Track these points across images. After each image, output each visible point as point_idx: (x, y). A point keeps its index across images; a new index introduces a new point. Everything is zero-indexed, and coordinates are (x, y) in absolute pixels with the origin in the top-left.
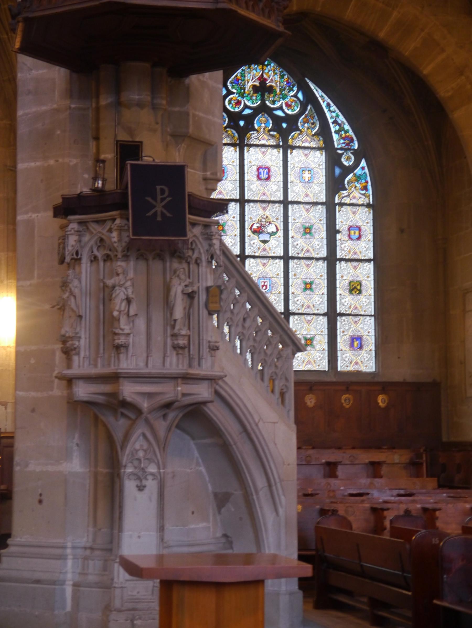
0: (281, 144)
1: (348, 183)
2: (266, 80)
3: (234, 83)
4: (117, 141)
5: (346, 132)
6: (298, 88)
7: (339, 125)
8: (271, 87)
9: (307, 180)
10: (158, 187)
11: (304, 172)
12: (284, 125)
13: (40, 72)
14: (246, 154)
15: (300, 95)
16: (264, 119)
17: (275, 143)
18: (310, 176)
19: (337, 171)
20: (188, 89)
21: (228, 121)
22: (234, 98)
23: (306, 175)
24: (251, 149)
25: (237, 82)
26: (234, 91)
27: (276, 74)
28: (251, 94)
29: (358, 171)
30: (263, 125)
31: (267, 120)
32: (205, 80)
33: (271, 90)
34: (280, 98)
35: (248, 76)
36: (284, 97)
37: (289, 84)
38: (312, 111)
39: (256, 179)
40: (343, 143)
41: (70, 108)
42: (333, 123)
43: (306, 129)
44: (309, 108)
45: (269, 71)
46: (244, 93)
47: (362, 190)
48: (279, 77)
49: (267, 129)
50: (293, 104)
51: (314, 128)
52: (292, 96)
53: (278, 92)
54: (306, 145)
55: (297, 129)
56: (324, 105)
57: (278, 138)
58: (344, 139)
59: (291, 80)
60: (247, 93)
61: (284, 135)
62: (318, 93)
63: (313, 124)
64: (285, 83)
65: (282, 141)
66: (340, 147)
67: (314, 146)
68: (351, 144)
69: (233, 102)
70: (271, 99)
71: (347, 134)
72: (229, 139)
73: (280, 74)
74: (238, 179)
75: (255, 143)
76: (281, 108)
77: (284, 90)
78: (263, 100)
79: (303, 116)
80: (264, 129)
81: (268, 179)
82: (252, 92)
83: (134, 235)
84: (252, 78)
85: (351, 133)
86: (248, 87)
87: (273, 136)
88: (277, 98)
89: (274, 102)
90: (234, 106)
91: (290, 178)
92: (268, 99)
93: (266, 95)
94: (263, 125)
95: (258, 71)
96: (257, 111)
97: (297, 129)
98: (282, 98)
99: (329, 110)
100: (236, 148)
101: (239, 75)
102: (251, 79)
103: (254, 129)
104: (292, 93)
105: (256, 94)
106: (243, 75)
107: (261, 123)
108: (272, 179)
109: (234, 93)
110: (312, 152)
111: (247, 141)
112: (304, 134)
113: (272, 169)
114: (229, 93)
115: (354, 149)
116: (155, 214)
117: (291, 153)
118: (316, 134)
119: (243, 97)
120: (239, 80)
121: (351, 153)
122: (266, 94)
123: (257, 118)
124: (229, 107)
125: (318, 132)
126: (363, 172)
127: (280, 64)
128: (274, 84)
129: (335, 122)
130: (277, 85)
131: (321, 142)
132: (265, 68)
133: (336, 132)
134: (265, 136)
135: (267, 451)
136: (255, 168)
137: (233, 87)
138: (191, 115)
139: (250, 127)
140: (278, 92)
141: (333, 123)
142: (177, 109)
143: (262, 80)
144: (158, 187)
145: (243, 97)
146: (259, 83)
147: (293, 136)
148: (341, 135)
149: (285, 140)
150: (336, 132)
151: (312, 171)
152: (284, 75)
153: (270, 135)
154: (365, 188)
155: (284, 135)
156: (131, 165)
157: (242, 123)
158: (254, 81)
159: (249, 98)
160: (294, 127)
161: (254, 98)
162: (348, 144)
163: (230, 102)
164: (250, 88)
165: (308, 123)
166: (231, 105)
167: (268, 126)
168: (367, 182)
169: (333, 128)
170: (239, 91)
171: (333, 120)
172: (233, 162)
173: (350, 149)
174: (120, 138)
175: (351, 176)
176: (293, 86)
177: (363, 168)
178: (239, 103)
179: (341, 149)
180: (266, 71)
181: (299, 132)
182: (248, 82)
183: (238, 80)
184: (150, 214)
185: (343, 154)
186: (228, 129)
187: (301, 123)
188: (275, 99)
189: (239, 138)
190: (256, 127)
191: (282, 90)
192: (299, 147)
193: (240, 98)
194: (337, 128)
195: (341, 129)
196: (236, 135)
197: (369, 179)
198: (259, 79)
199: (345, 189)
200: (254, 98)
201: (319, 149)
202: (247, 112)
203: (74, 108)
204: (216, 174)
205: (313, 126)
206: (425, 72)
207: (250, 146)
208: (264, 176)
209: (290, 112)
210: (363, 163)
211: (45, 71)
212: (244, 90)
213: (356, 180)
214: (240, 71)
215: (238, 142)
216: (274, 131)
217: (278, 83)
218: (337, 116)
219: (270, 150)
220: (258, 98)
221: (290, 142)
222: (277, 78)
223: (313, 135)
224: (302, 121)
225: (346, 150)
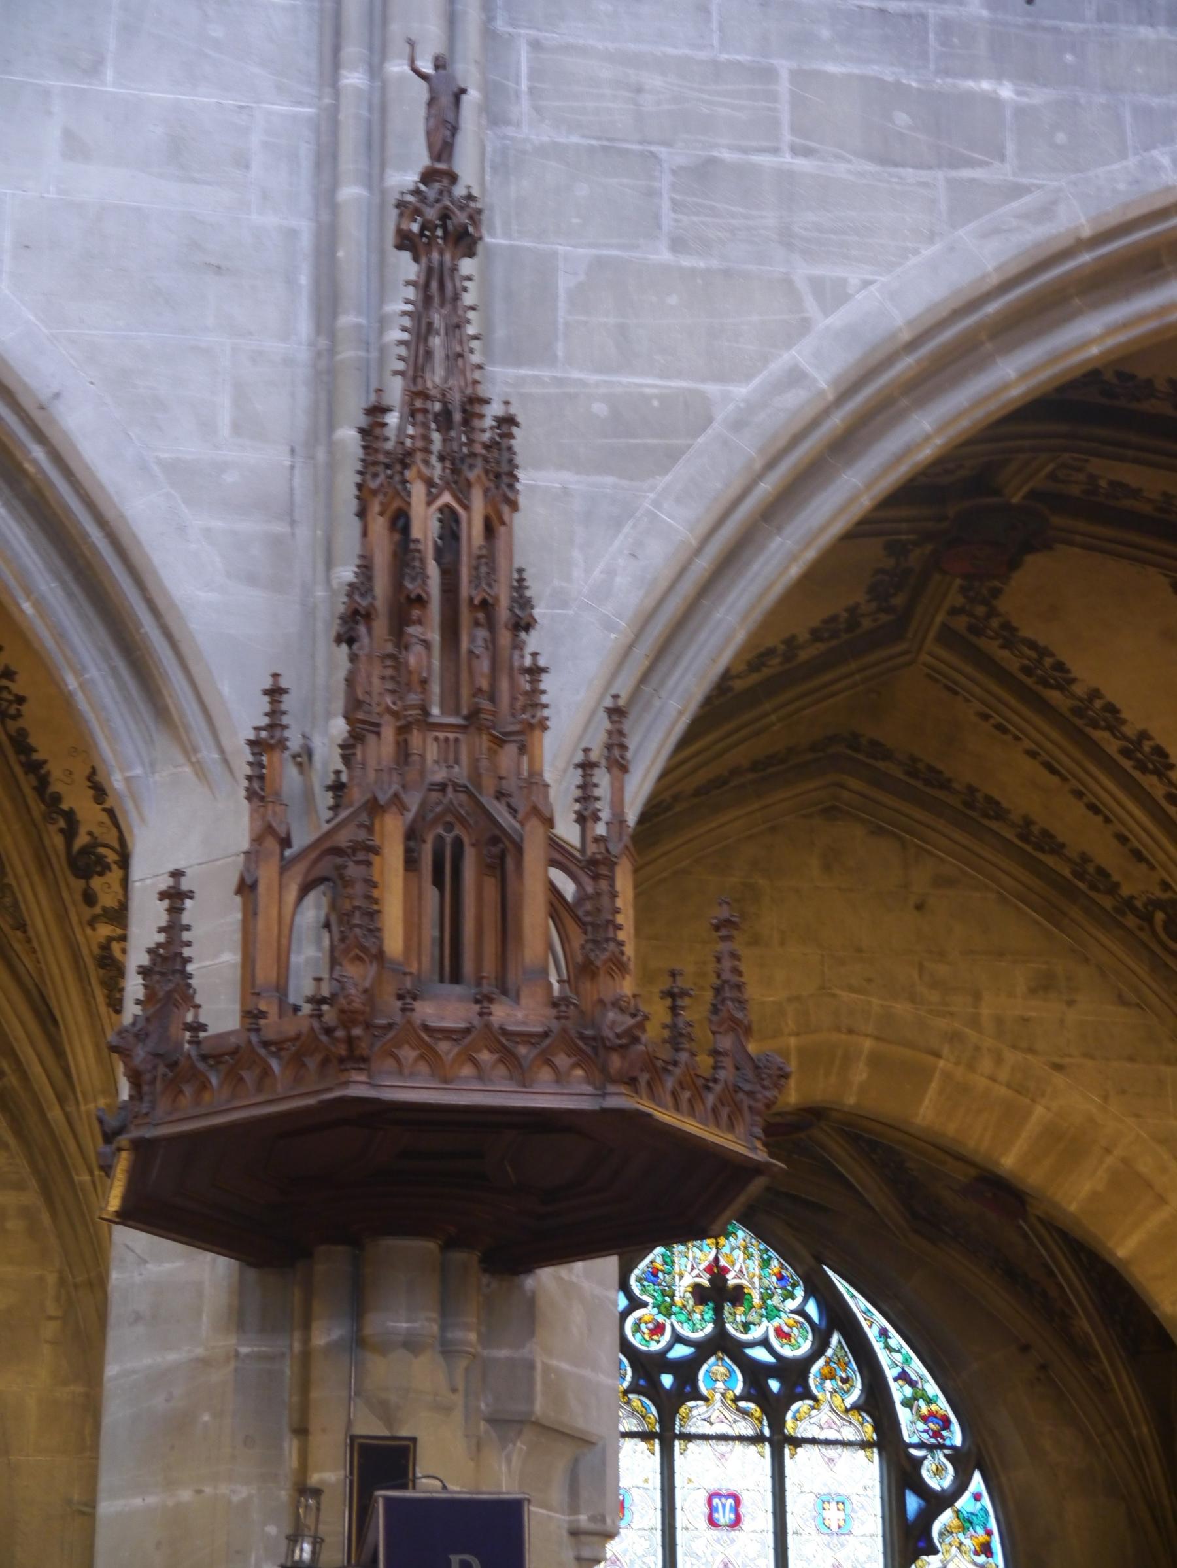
0: (767, 1432)
1: (941, 1534)
2: (725, 1270)
3: (646, 1280)
4: (353, 1438)
5: (929, 1401)
6: (805, 1291)
7: (912, 1384)
8: (739, 1288)
9: (835, 1528)
11: (826, 1506)
12: (774, 1385)
13: (167, 1266)
14: (679, 1460)
15: (812, 1309)
16: (722, 1370)
17: (750, 1432)
18: (841, 1515)
19: (913, 1503)
20: (531, 1303)
21: (633, 1378)
22: (647, 1318)
23: (833, 1515)
24: (691, 1445)
25: (652, 1278)
26: (645, 1298)
27: (750, 1256)
28: (689, 1308)
29: (965, 1503)
30: (720, 1385)
31: (731, 1372)
32: (574, 1279)
33: (738, 1296)
34: (762, 1316)
36: (771, 1313)
37: (783, 1282)
38: (842, 1347)
39: (703, 1523)
40: (925, 1431)
41: (237, 1354)
42: (896, 1379)
43: (828, 1394)
44: (836, 1338)
45: (733, 1249)
46: (673, 1303)
47: (976, 1553)
48: (757, 1263)
49: (730, 1395)
50: (795, 1331)
51: (848, 1392)
52: (792, 1312)
53: (756, 1301)
54: (832, 1435)
55: (808, 1395)
56: (872, 1334)
57: (757, 1419)
58: (925, 1419)
59: (789, 1272)
60: (679, 1304)
61: (774, 1409)
62: (858, 1304)
63: (845, 1381)
64: (774, 1279)
65: (770, 1426)
66: (915, 1440)
67: (852, 1438)
68: (944, 1433)
69: (643, 1326)
70: (738, 1318)
71: (934, 1407)
72: (634, 1421)
73: (762, 1257)
74: (659, 1526)
75: (701, 1431)
76: (765, 1343)
77: (771, 1297)
78: (719, 1321)
79: (821, 1362)
80: (723, 1395)
81: (736, 1523)
82: (691, 1302)
84: (693, 1266)
85: (943, 1405)
86: (682, 1289)
87: (745, 1413)
88: (753, 1317)
89: (746, 1327)
90: (647, 1337)
91: (791, 1523)
92: (731, 1319)
93: (726, 1308)
94: (720, 1385)
95: (706, 1248)
96: (705, 1349)
97: (808, 1395)
98: (767, 1318)
99: (887, 1347)
100: (653, 1445)
101: (659, 1260)
102: (689, 1268)
103: (698, 1396)
104: (791, 1305)
105: (701, 1307)
106: (669, 1262)
107: (717, 1380)
108: (746, 1523)
109: (645, 1305)
110: (847, 1453)
111: (681, 1426)
112: (825, 1408)
113: (746, 1498)
114: (635, 1304)
115: (953, 1447)
117: (793, 1456)
118: (856, 1407)
119: (669, 1315)
120: (658, 1270)
121: (946, 1456)
122: (727, 1307)
123: (705, 1367)
124: (636, 1341)
125: (861, 1402)
126: (978, 1505)
127: (759, 1233)
128: (744, 1282)
129: (903, 1377)
130: (752, 1283)
131: (869, 1428)
132: (722, 1240)
133: (907, 1403)
134: (726, 1413)
136: (702, 1497)
137: (644, 1290)
138: (539, 1366)
139: (687, 1389)
140: (756, 1301)
141: (896, 1379)
142: (503, 1353)
143: (717, 1272)
145: (669, 1315)
146: (709, 1280)
147: (798, 1411)
148: (919, 1410)
149: (777, 1423)
150: (907, 1403)
151: (847, 1503)
152: (770, 1258)
153: (738, 1409)
154: (986, 1549)
155: (774, 1409)
156: (388, 1500)
158: (698, 1276)
159: (683, 1318)
160: (799, 1390)
161: (697, 1317)
162: (936, 1434)
163: (637, 1328)
164: (686, 1291)
165: (832, 1378)
166: (638, 1335)
167: (730, 1385)
168: (989, 1533)
169: (899, 1391)
170: (660, 1299)
171: (896, 1371)
172: (646, 1481)
173: (942, 1447)
174: (360, 1429)
175: (946, 1518)
176: (794, 1286)
177: (977, 1497)
178: (658, 1329)
179: (921, 1445)
180: (726, 1250)
181: (811, 1402)
182: (681, 1276)
183: (655, 1273)
185: (925, 1458)
186: (630, 1396)
187: (816, 1377)
188: (750, 1319)
189: (661, 1421)
190: (703, 1388)
191: (766, 1296)
192: (814, 1441)
193: (661, 1319)
194: (908, 1391)
195: (920, 1394)
196: (654, 1410)
197: (993, 1525)
198: (709, 1269)
199: (935, 1552)
200: (697, 1317)
201: (864, 1445)
203: (247, 1356)
204: (603, 1520)
205: (845, 1387)
206: (1122, 1252)
207: (688, 1438)
208: (725, 1516)
209: (787, 1352)
210: (977, 1482)
211: (178, 1264)
212: (672, 1296)
213: (959, 1527)
215: (658, 1429)
216: (747, 1400)
217: (756, 1280)
218: (907, 1360)
219: (738, 1446)
220: (707, 1317)
221: (790, 1427)
222: (754, 1266)
223: (847, 1411)
224: (818, 1375)
225: (931, 1448)
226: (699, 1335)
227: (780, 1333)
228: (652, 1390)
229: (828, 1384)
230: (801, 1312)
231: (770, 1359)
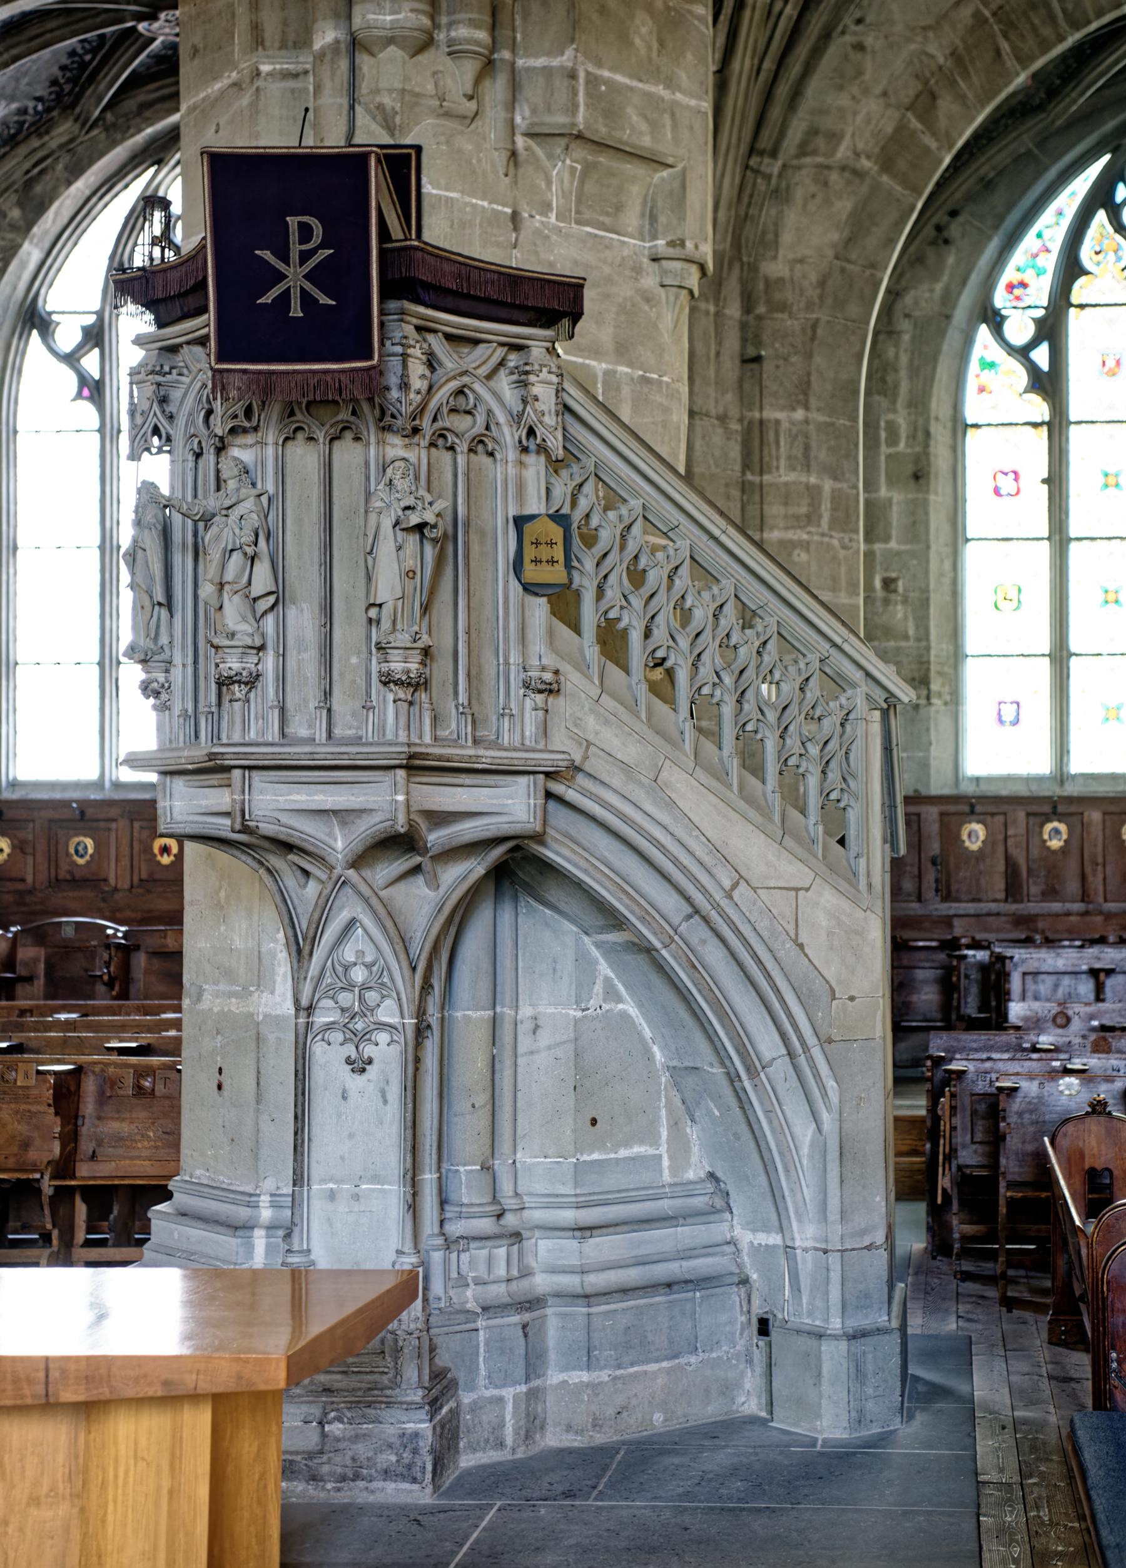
10: (292, 221)
83: (220, 359)
116: (284, 298)
135: (770, 964)
144: (292, 221)
184: (267, 299)
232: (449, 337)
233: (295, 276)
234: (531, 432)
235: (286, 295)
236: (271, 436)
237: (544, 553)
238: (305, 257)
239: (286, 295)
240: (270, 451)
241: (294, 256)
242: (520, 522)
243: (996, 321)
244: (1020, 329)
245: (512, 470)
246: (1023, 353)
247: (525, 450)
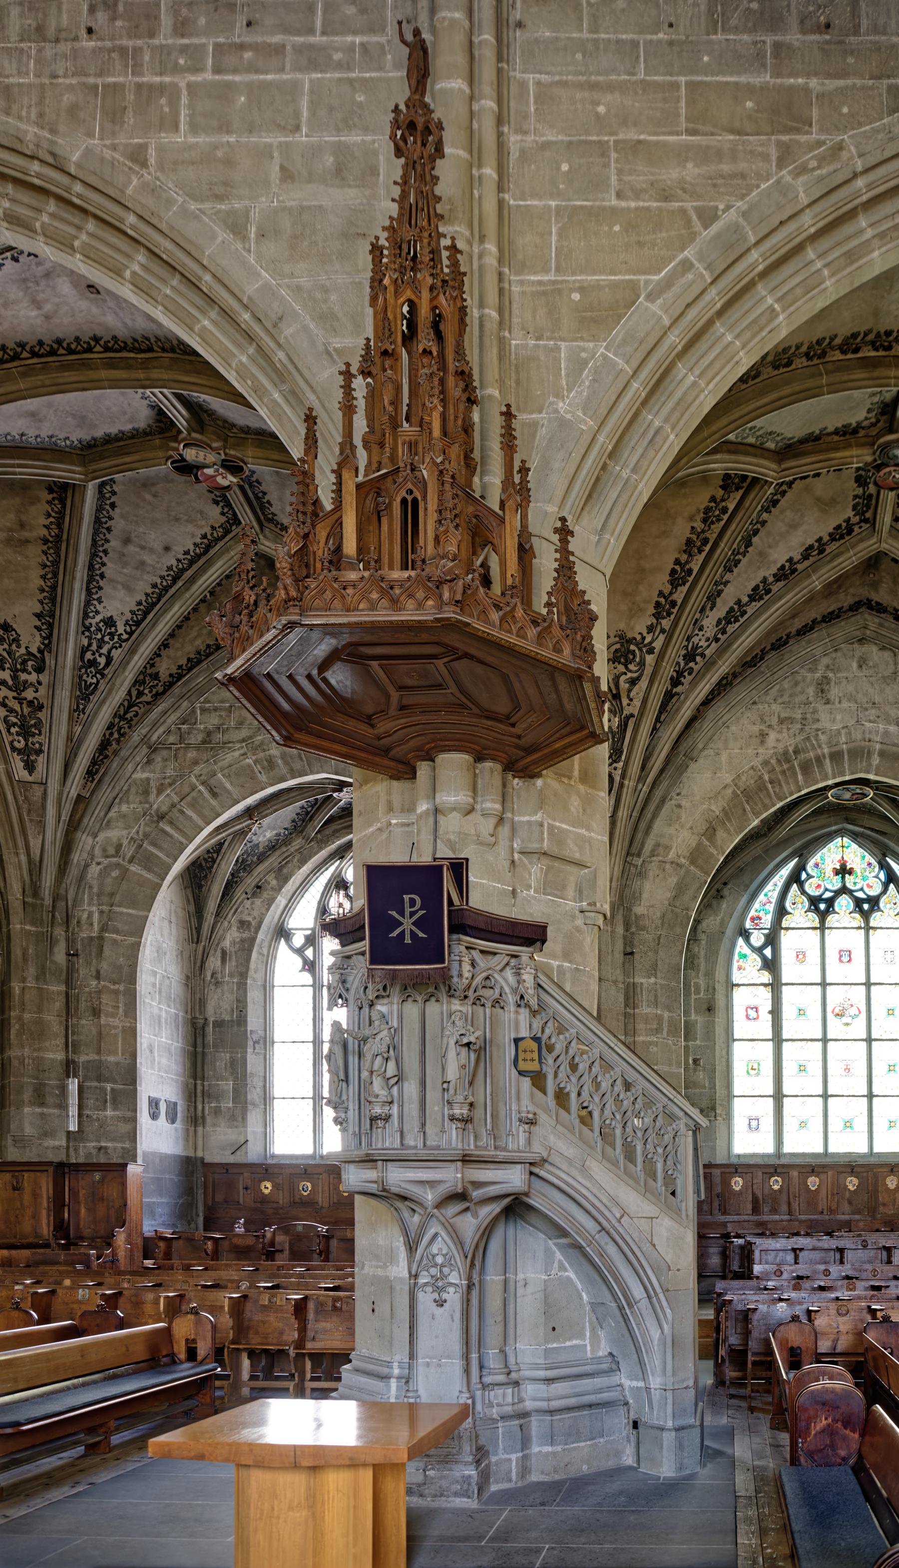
8: (851, 869)
12: (866, 906)
15: (882, 876)
33: (851, 872)
35: (828, 860)
36: (864, 878)
59: (873, 861)
61: (866, 915)
76: (862, 889)
83: (371, 963)
89: (855, 883)
96: (838, 893)
112: (886, 914)
114: (810, 877)
149: (867, 921)
155: (866, 915)
157: (822, 906)
184: (395, 934)
202: (828, 895)
214: (819, 854)
221: (872, 923)
222: (858, 859)
226: (835, 888)
227: (869, 886)
228: (817, 910)
229: (888, 906)
230: (877, 877)
231: (864, 896)
232: (482, 952)
233: (407, 924)
234: (522, 997)
235: (403, 932)
236: (396, 998)
237: (529, 1056)
238: (412, 914)
239: (403, 932)
240: (395, 1007)
241: (407, 914)
242: (517, 1041)
243: (745, 934)
244: (757, 939)
245: (512, 1016)
246: (759, 950)
247: (519, 1006)
